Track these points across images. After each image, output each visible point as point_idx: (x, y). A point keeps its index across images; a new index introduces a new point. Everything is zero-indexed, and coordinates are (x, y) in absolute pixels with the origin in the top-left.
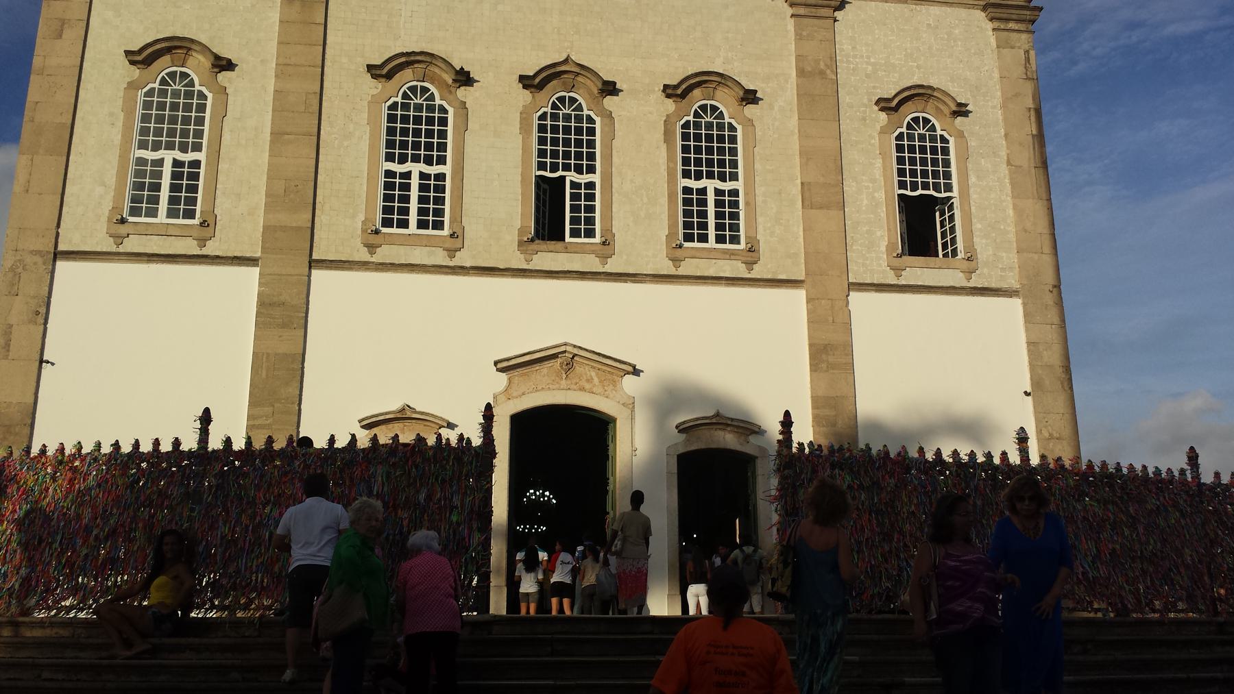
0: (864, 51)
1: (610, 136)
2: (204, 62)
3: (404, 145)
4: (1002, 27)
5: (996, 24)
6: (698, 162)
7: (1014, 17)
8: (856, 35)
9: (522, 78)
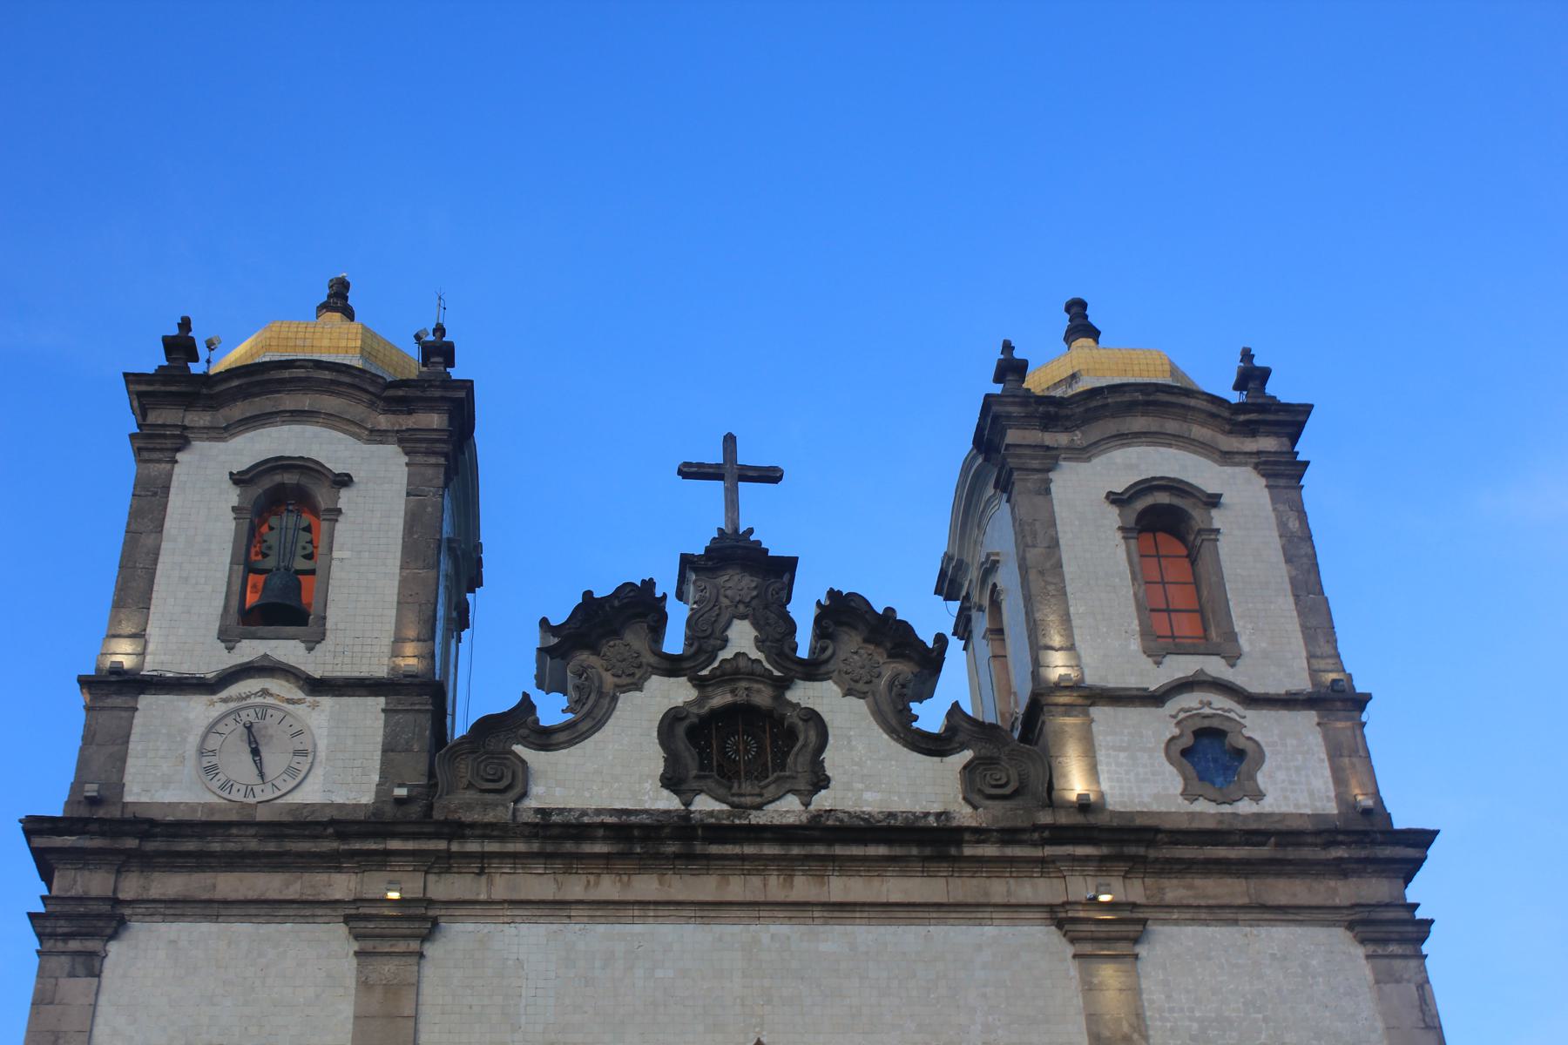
0: (1184, 1001)
4: (1380, 951)
5: (1370, 949)
7: (1393, 936)
8: (1170, 978)
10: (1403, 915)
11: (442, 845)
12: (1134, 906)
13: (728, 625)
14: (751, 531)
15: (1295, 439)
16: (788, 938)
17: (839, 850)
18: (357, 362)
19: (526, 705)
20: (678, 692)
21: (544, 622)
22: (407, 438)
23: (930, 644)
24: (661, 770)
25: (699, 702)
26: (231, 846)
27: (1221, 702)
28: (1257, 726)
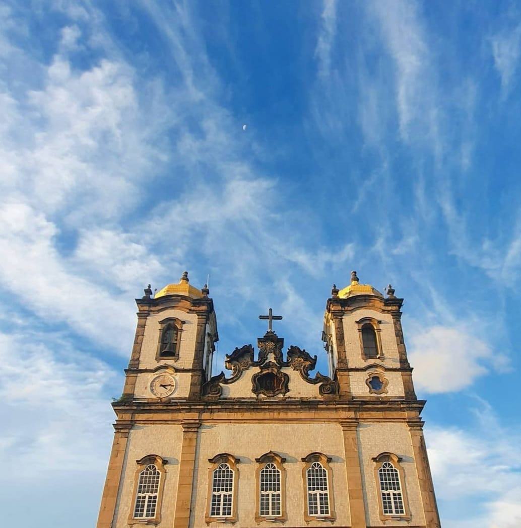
1: (285, 476)
2: (160, 461)
3: (219, 485)
6: (314, 484)
9: (256, 459)
10: (418, 420)
11: (203, 407)
12: (357, 419)
13: (268, 354)
14: (274, 332)
15: (400, 307)
16: (278, 427)
17: (290, 407)
18: (187, 294)
19: (222, 374)
20: (257, 370)
21: (227, 355)
22: (198, 313)
23: (313, 358)
24: (252, 388)
25: (261, 372)
26: (156, 408)
27: (379, 370)
28: (388, 376)
